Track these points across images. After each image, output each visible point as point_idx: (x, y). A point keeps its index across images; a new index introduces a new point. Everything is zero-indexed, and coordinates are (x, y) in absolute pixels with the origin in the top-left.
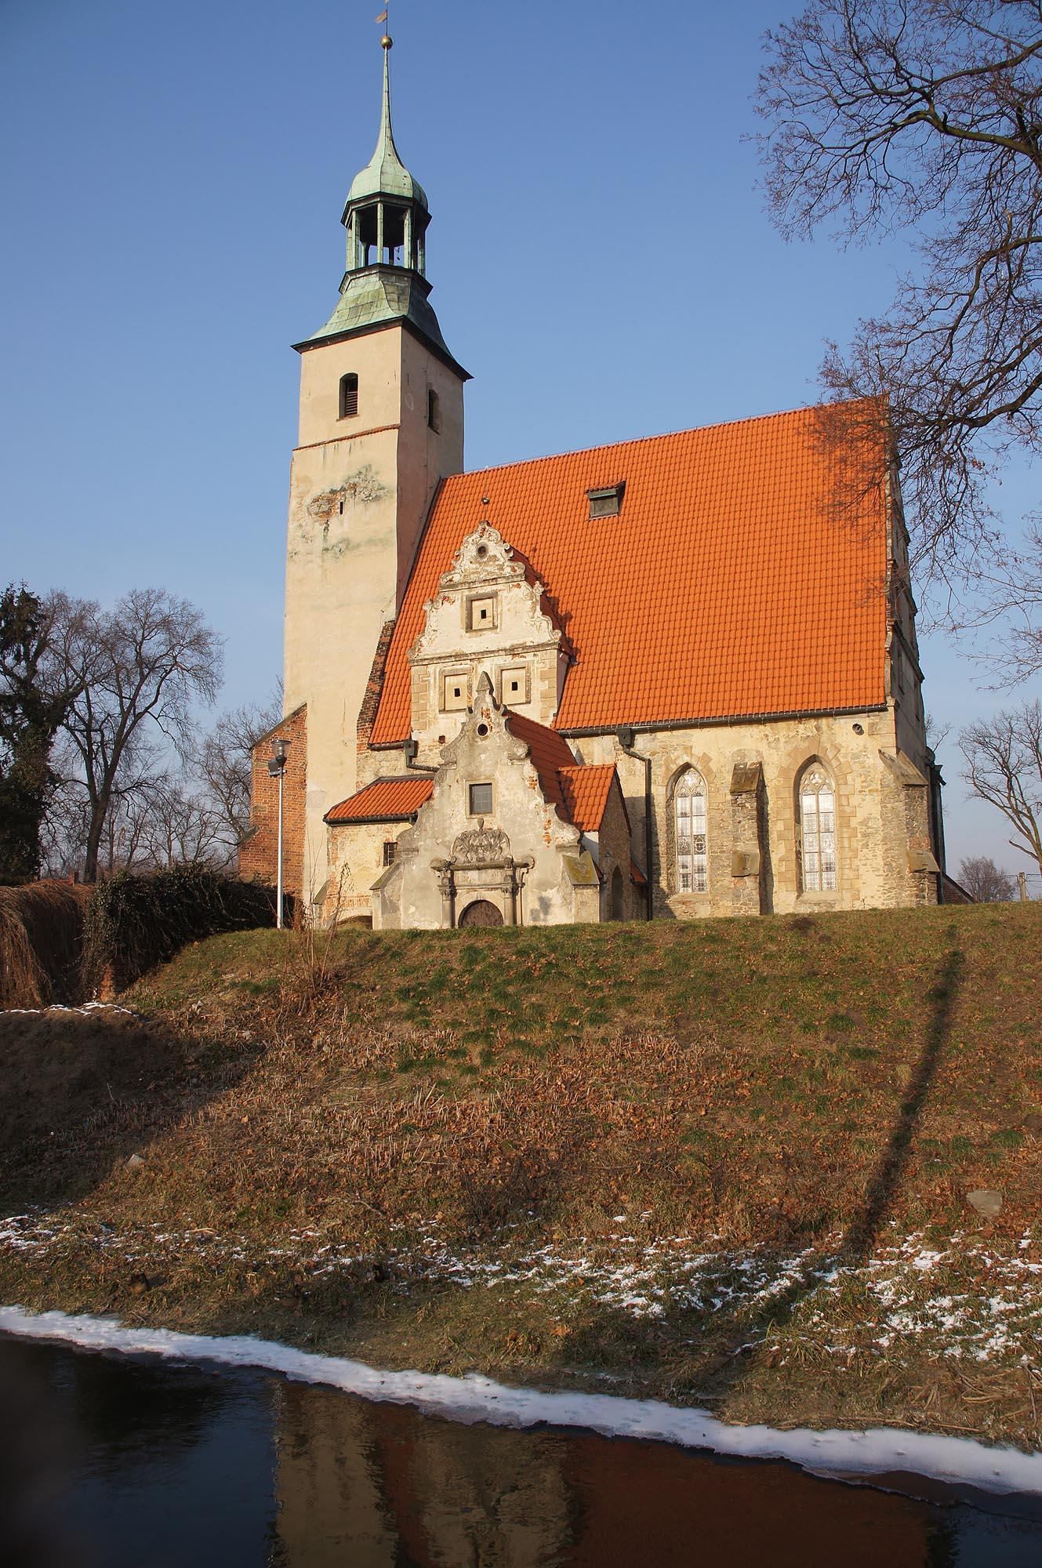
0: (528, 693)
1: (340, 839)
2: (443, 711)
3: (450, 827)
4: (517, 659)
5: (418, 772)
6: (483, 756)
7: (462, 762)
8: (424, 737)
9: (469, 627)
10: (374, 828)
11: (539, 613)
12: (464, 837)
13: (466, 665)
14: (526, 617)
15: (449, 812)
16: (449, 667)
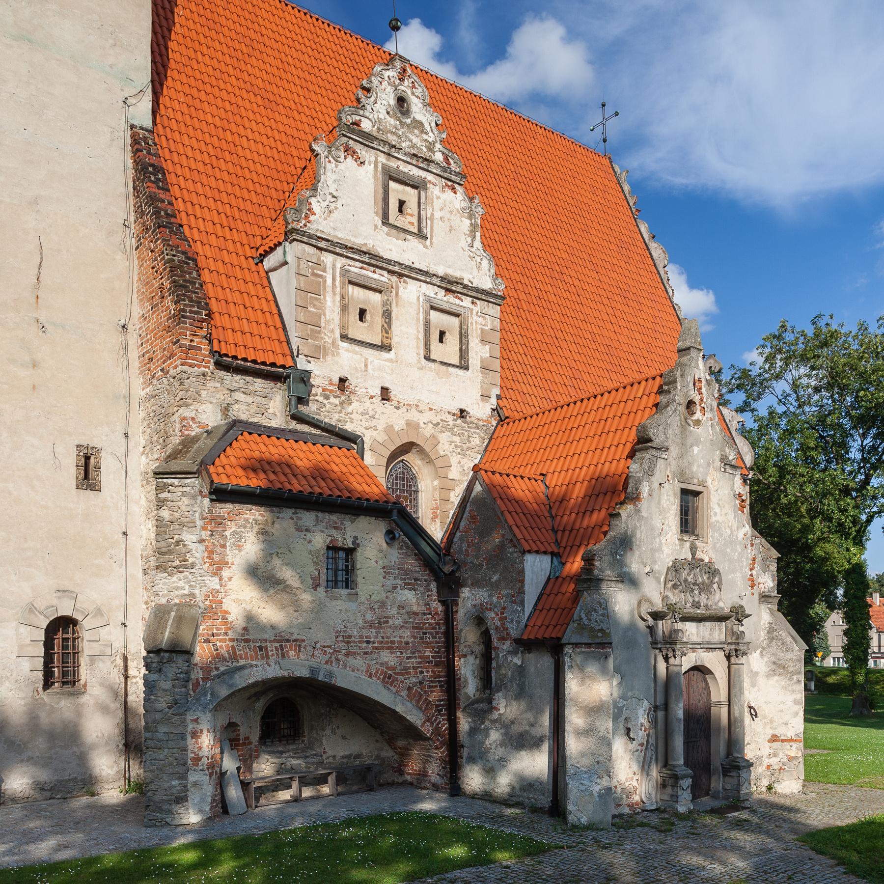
0: (464, 353)
1: (231, 528)
2: (344, 337)
3: (659, 550)
4: (451, 298)
5: (305, 428)
6: (696, 449)
7: (674, 451)
8: (322, 373)
9: (385, 220)
10: (308, 518)
11: (478, 244)
12: (676, 567)
13: (380, 277)
14: (464, 241)
15: (658, 525)
16: (355, 269)
